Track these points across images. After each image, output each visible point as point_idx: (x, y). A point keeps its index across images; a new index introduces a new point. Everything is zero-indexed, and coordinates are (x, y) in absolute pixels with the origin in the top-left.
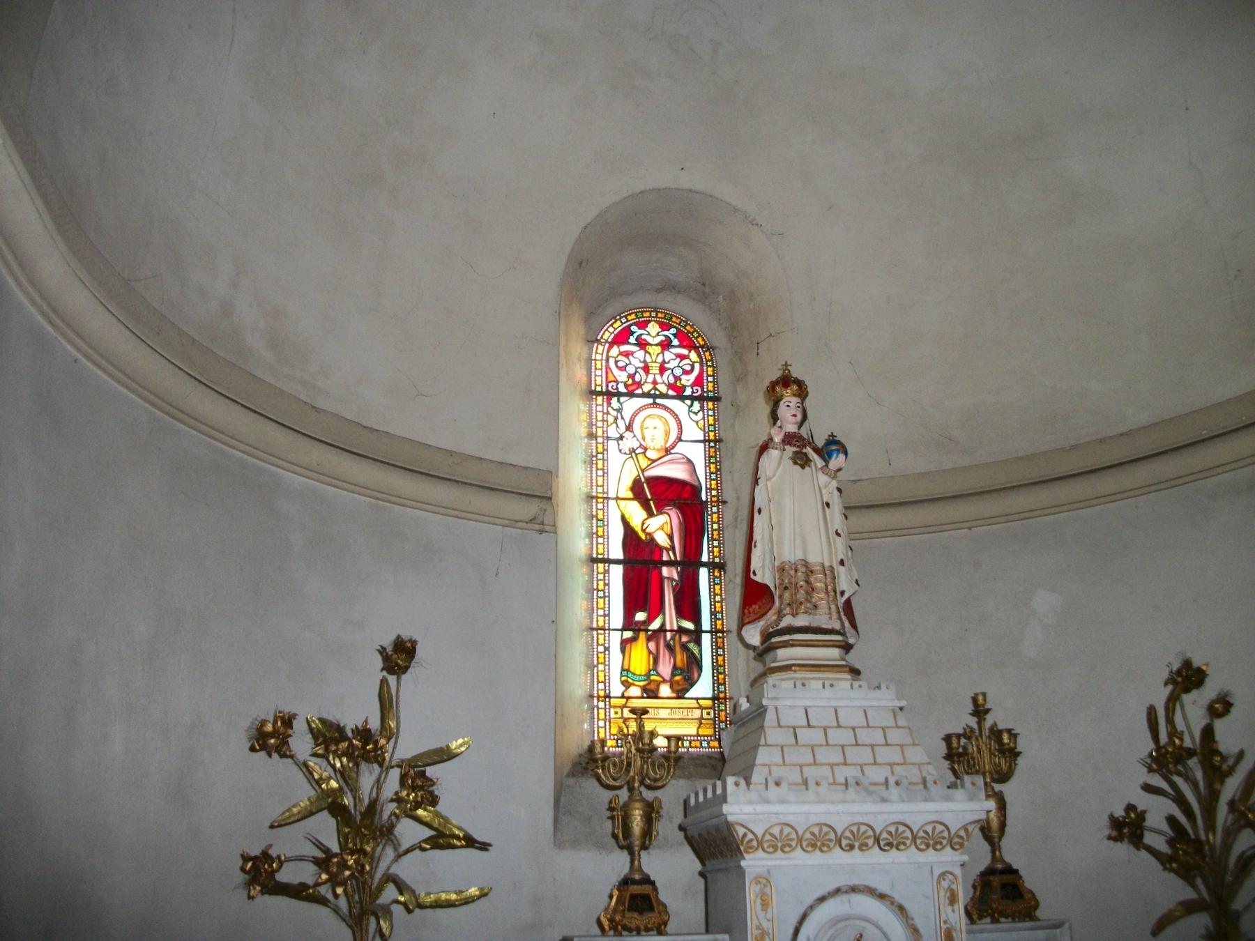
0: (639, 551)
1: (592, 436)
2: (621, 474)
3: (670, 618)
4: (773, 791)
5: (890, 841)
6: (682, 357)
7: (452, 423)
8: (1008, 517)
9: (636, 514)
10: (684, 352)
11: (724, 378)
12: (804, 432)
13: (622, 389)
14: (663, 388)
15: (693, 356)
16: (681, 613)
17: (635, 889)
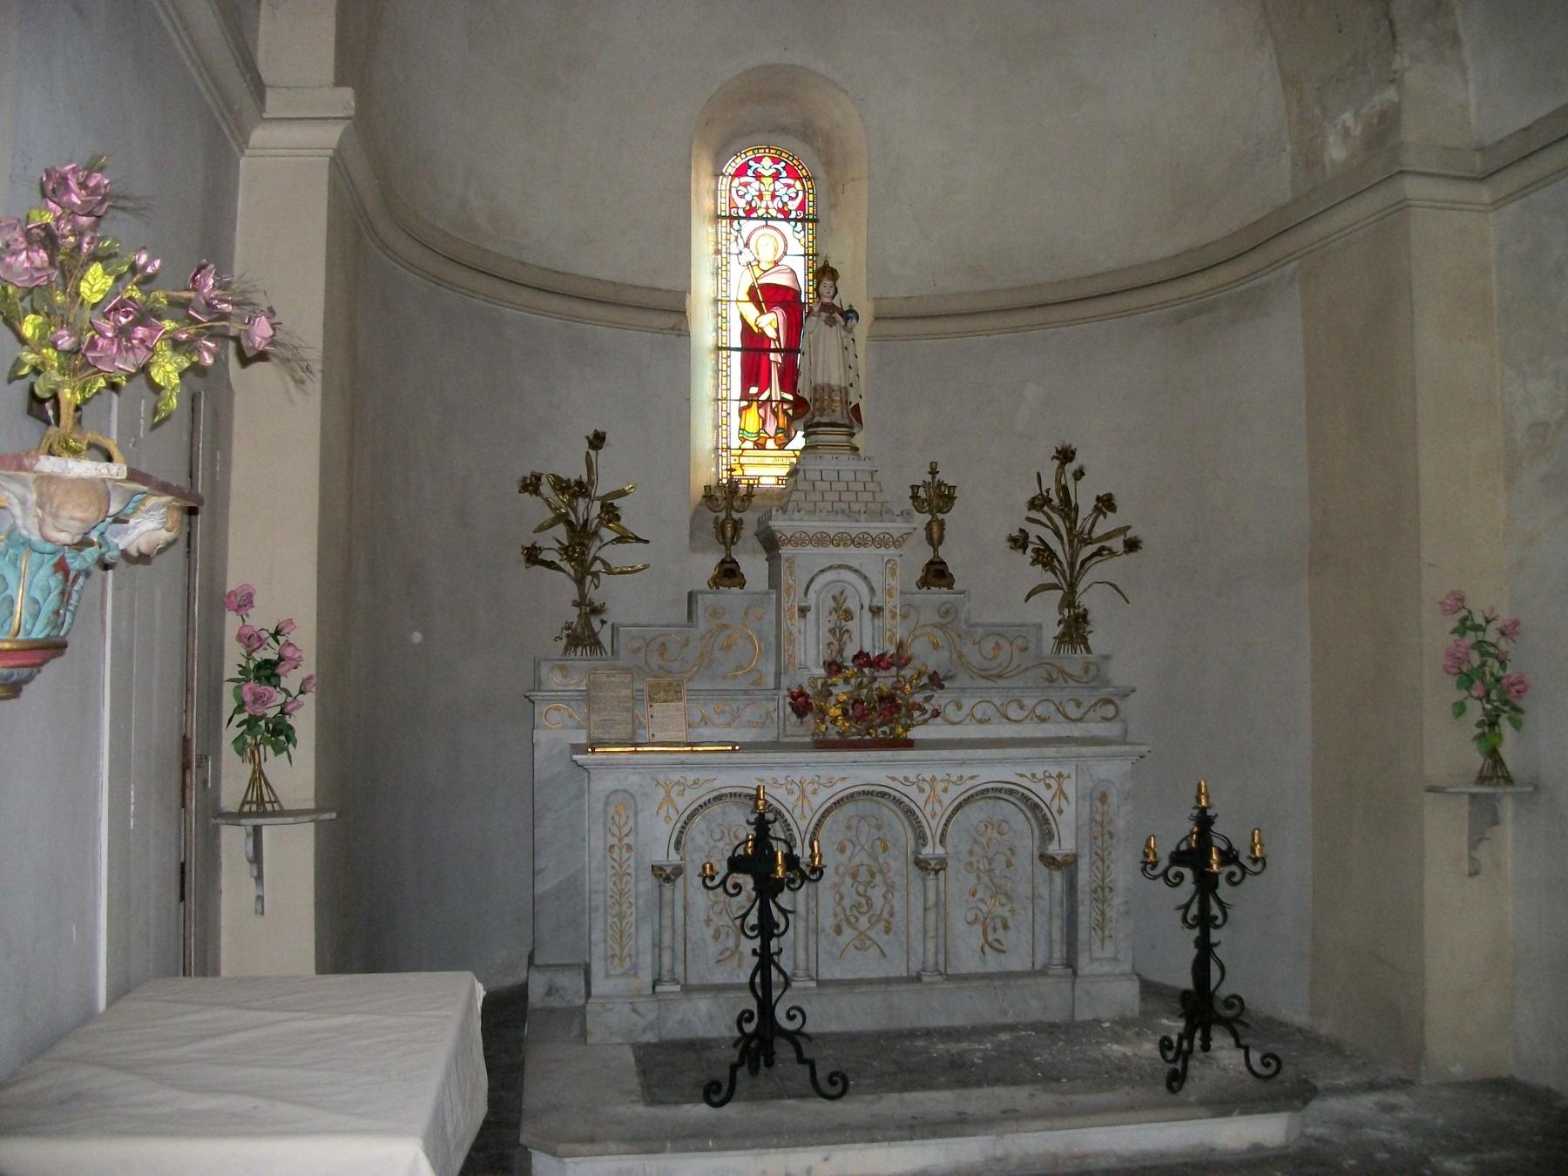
0: (754, 344)
1: (718, 252)
2: (740, 282)
3: (775, 391)
4: (796, 515)
5: (860, 541)
6: (789, 186)
7: (616, 261)
8: (1015, 329)
9: (751, 312)
10: (791, 181)
11: (822, 203)
12: (836, 302)
13: (742, 214)
14: (773, 213)
15: (798, 185)
16: (783, 388)
17: (727, 566)
